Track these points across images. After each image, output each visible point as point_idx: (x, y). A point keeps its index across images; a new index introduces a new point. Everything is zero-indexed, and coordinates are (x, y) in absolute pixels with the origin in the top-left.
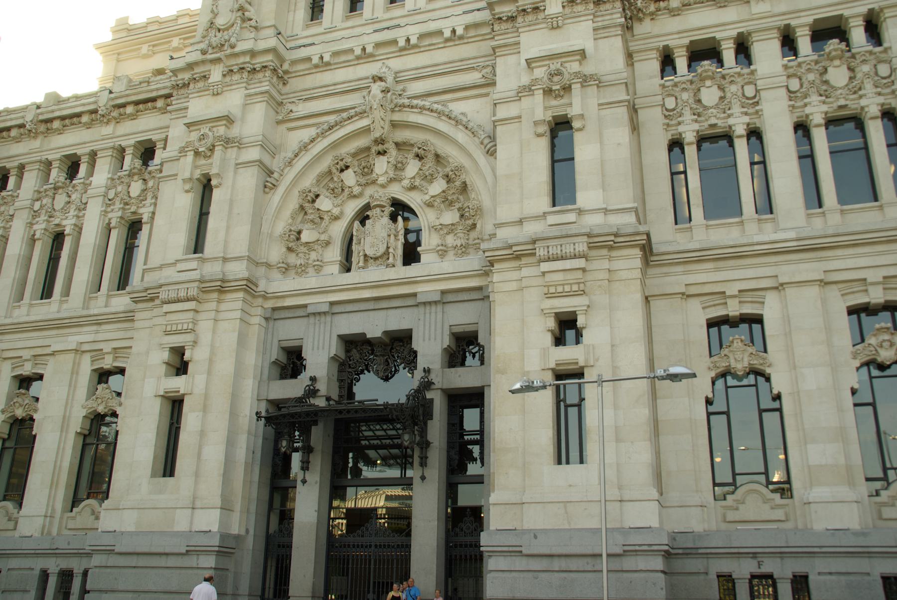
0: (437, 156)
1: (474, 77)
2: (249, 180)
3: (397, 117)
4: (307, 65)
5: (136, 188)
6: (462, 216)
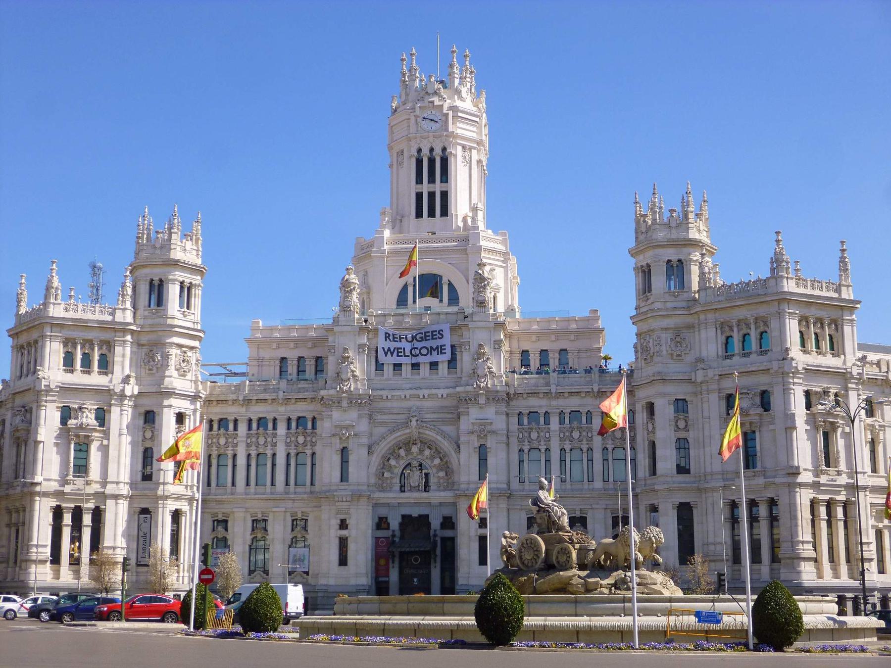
0: (436, 449)
2: (364, 451)
3: (421, 431)
5: (301, 439)
6: (446, 474)
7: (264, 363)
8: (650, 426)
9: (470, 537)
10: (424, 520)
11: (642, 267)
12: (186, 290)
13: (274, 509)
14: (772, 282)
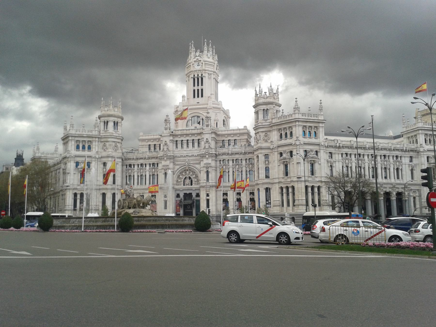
1: (198, 162)
3: (189, 166)
5: (153, 170)
7: (144, 147)
8: (258, 163)
12: (116, 124)
13: (146, 192)
14: (293, 115)
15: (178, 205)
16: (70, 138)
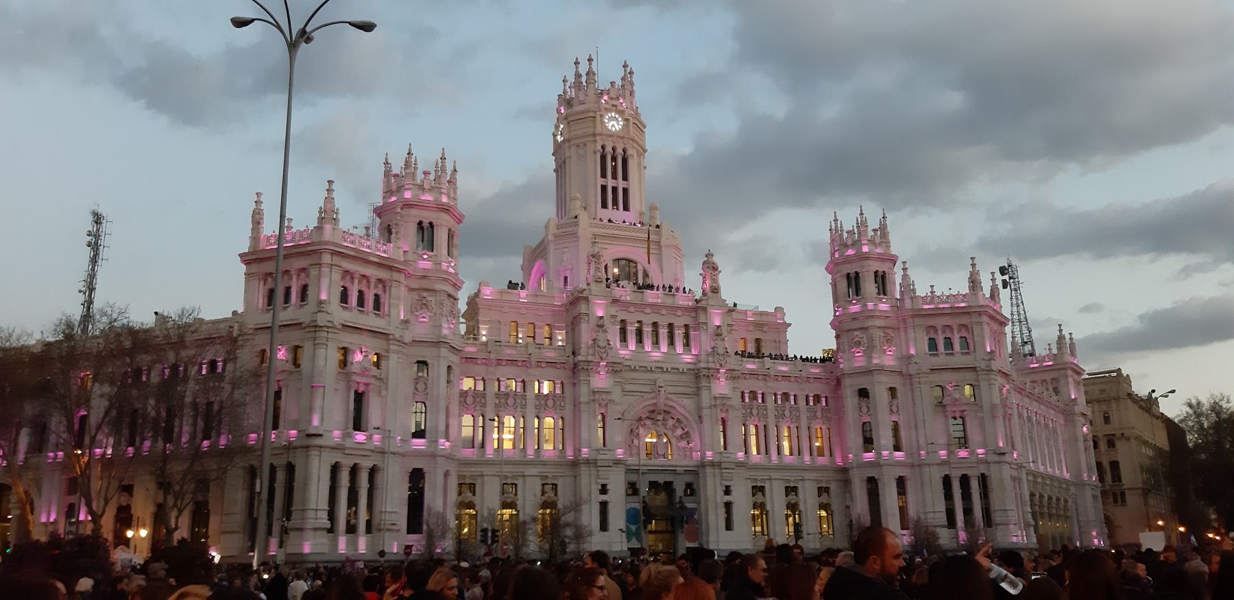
4: (628, 368)
8: (864, 409)
9: (716, 503)
10: (668, 487)
11: (848, 274)
15: (639, 518)
16: (327, 258)
